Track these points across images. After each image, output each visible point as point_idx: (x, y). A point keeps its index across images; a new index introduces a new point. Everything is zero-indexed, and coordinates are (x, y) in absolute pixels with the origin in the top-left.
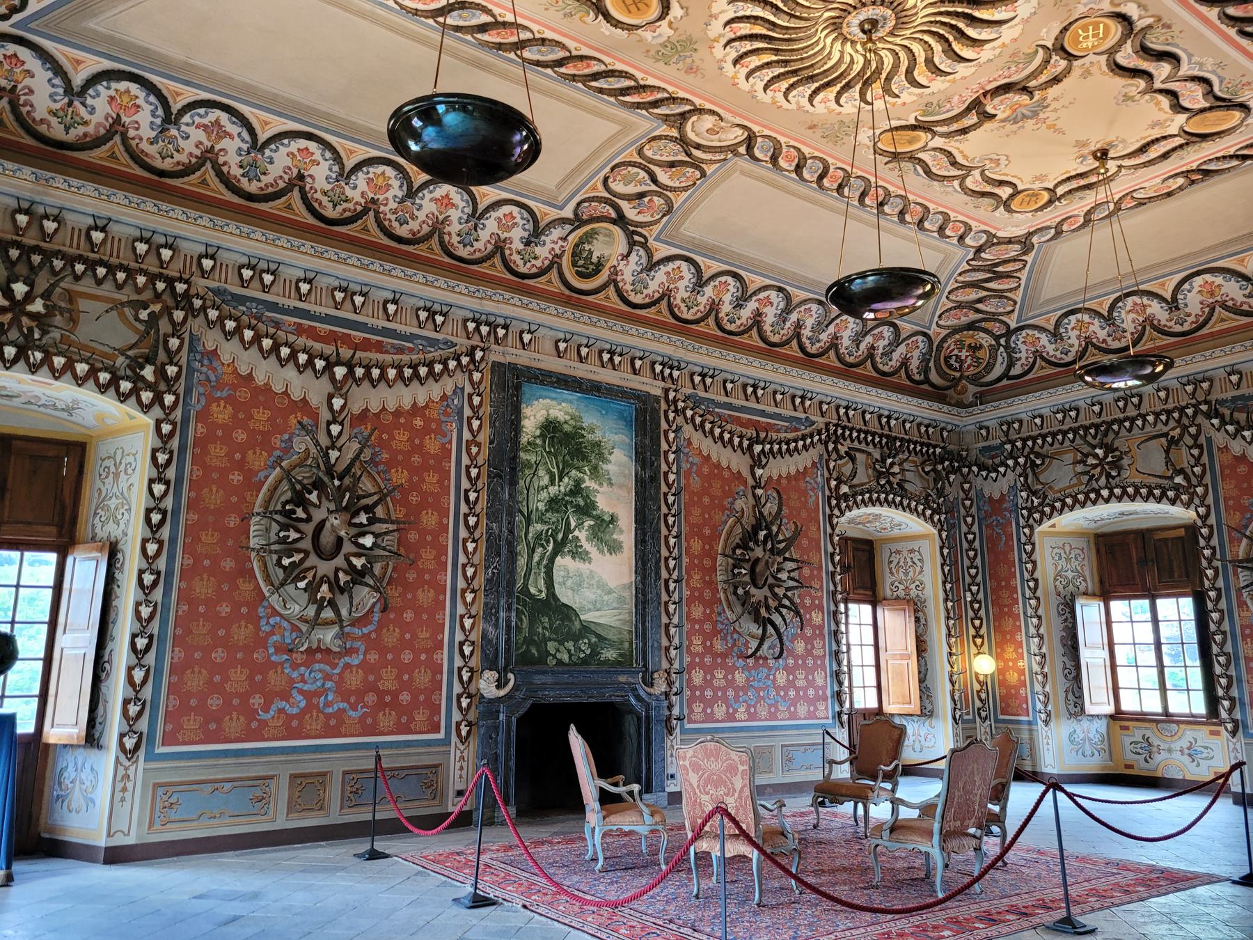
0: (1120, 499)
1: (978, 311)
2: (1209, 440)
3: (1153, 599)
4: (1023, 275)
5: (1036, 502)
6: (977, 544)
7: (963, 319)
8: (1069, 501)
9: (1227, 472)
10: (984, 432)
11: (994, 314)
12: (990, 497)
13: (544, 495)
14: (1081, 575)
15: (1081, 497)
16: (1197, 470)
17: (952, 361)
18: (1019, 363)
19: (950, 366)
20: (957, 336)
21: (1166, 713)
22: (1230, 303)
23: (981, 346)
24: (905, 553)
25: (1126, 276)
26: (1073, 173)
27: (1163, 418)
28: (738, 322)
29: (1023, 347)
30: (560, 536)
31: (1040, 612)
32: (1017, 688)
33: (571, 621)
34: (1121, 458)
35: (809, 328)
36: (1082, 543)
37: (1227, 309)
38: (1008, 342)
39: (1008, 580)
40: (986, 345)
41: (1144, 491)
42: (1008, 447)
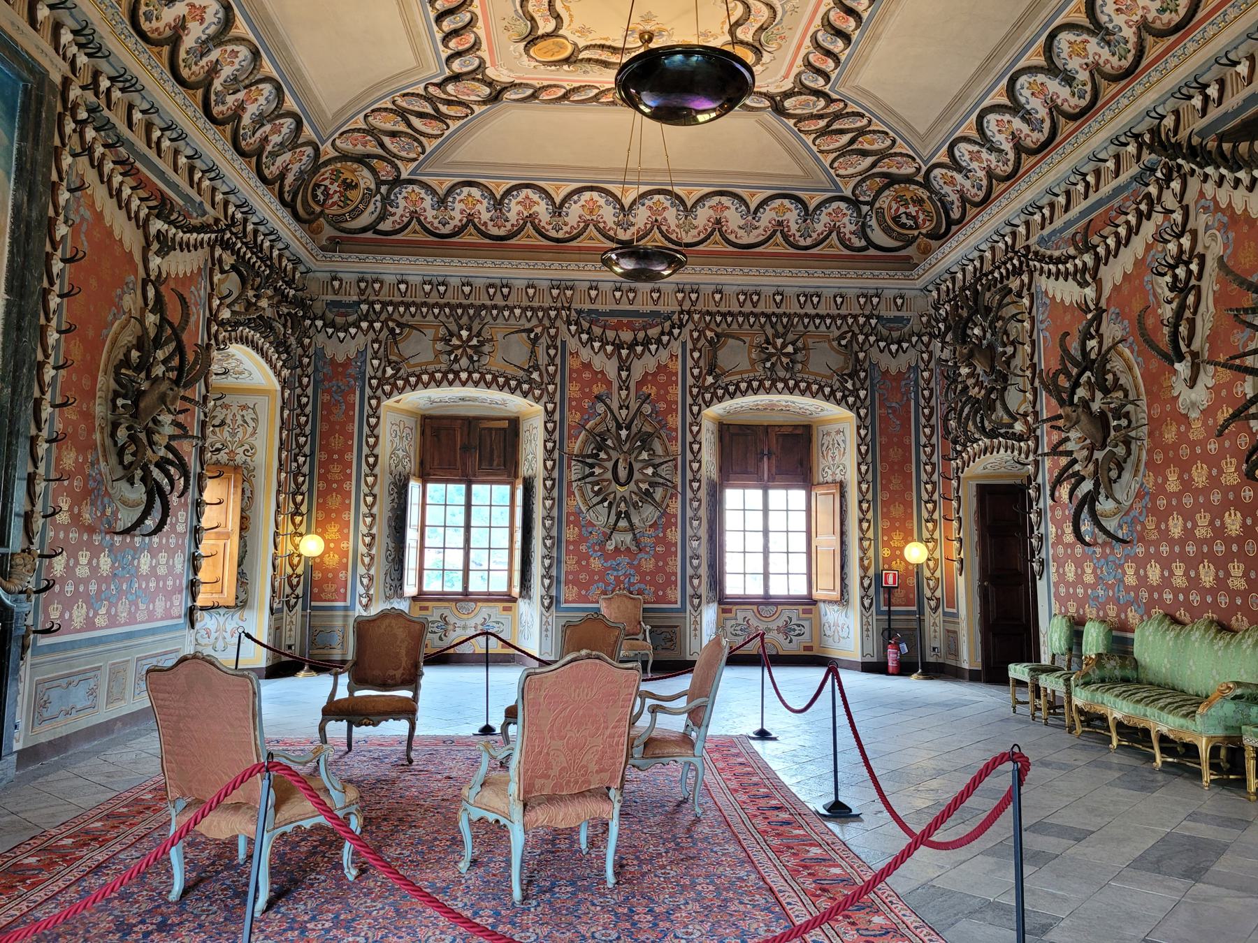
0: (476, 384)
1: (382, 145)
2: (564, 343)
3: (766, 490)
4: (454, 126)
5: (389, 371)
6: (308, 409)
7: (360, 147)
8: (425, 378)
9: (575, 375)
10: (336, 284)
11: (395, 156)
12: (332, 359)
14: (408, 456)
15: (438, 376)
16: (551, 369)
17: (319, 192)
18: (391, 219)
19: (315, 196)
20: (339, 165)
21: (466, 593)
22: (601, 225)
23: (357, 186)
24: (235, 409)
25: (633, 170)
26: (608, 43)
27: (529, 314)
28: (155, 24)
29: (402, 203)
31: (376, 490)
32: (335, 572)
34: (482, 344)
35: (221, 80)
36: (411, 422)
37: (598, 230)
38: (389, 191)
39: (342, 453)
40: (362, 186)
41: (501, 380)
42: (364, 307)
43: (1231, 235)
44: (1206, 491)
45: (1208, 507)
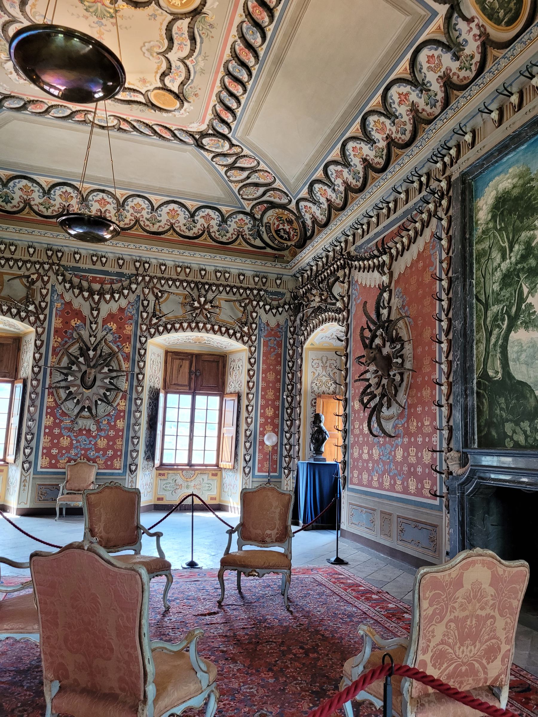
13: (498, 275)
30: (514, 309)
33: (525, 397)
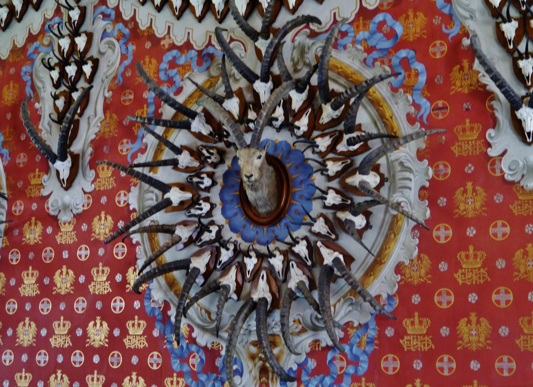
43: (132, 47)
44: (69, 298)
45: (69, 314)
